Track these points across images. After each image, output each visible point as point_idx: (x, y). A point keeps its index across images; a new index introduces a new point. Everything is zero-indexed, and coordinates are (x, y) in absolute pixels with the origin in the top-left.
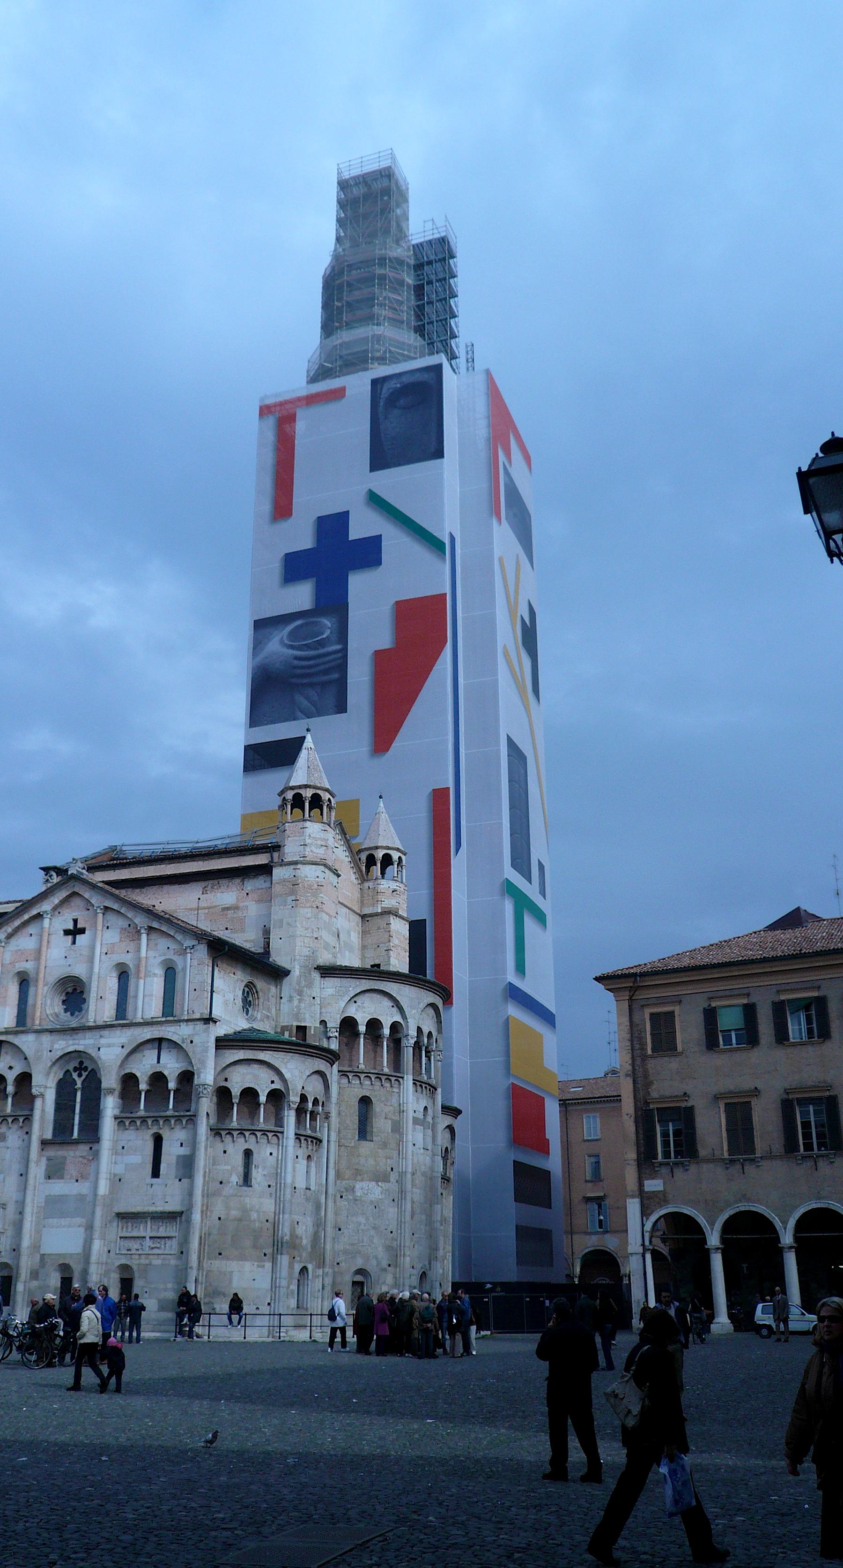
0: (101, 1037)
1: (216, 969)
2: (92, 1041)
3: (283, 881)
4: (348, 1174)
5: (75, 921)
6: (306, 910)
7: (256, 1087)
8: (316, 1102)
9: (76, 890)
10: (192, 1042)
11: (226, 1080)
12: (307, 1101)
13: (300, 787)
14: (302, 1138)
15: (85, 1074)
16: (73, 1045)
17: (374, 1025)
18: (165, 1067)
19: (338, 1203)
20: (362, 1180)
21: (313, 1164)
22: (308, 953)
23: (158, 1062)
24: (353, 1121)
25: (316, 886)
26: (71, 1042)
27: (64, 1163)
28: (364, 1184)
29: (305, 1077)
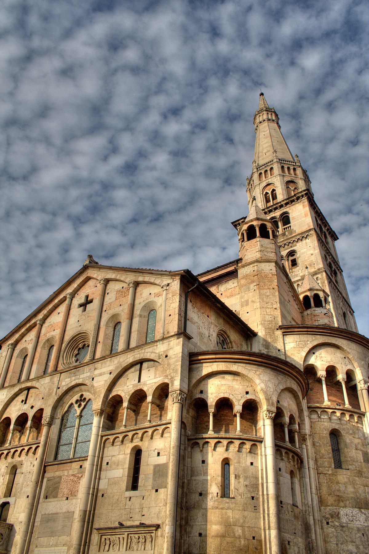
0: (95, 369)
1: (190, 305)
2: (88, 374)
3: (246, 277)
4: (330, 500)
5: (87, 297)
6: (265, 291)
7: (231, 397)
8: (292, 418)
9: (89, 275)
10: (166, 356)
11: (201, 392)
12: (284, 416)
13: (252, 221)
14: (284, 451)
15: (83, 404)
16: (75, 380)
17: (331, 371)
18: (145, 384)
19: (325, 530)
20: (345, 507)
21: (296, 481)
22: (270, 319)
23: (139, 381)
24: (326, 449)
25: (270, 275)
26: (73, 378)
27: (59, 483)
28: (348, 511)
29: (279, 391)
